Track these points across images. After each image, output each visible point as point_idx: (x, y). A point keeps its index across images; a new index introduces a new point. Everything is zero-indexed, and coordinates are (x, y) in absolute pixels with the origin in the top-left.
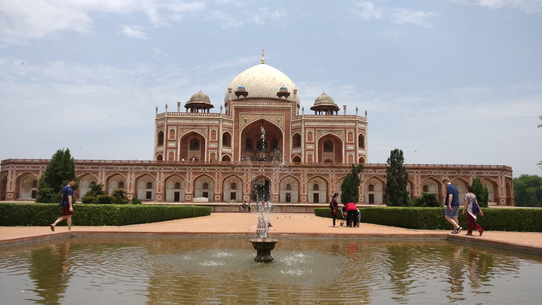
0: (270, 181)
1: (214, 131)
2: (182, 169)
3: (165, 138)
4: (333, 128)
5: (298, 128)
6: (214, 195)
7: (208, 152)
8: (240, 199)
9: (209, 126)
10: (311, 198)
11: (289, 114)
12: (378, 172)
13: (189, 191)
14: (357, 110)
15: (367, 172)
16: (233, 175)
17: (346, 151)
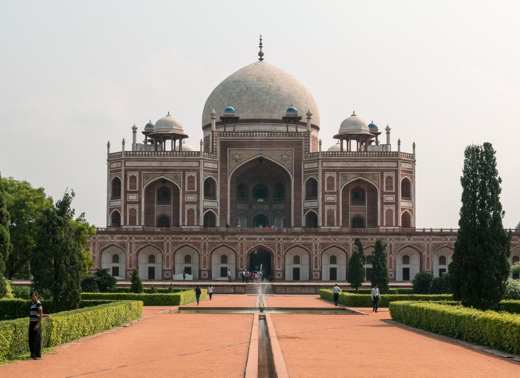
0: (273, 253)
1: (191, 177)
2: (159, 239)
3: (122, 188)
4: (365, 171)
5: (313, 171)
6: (200, 271)
8: (233, 276)
9: (184, 171)
10: (326, 274)
11: (301, 149)
12: (414, 240)
13: (168, 266)
15: (399, 239)
16: (224, 245)
17: (383, 203)
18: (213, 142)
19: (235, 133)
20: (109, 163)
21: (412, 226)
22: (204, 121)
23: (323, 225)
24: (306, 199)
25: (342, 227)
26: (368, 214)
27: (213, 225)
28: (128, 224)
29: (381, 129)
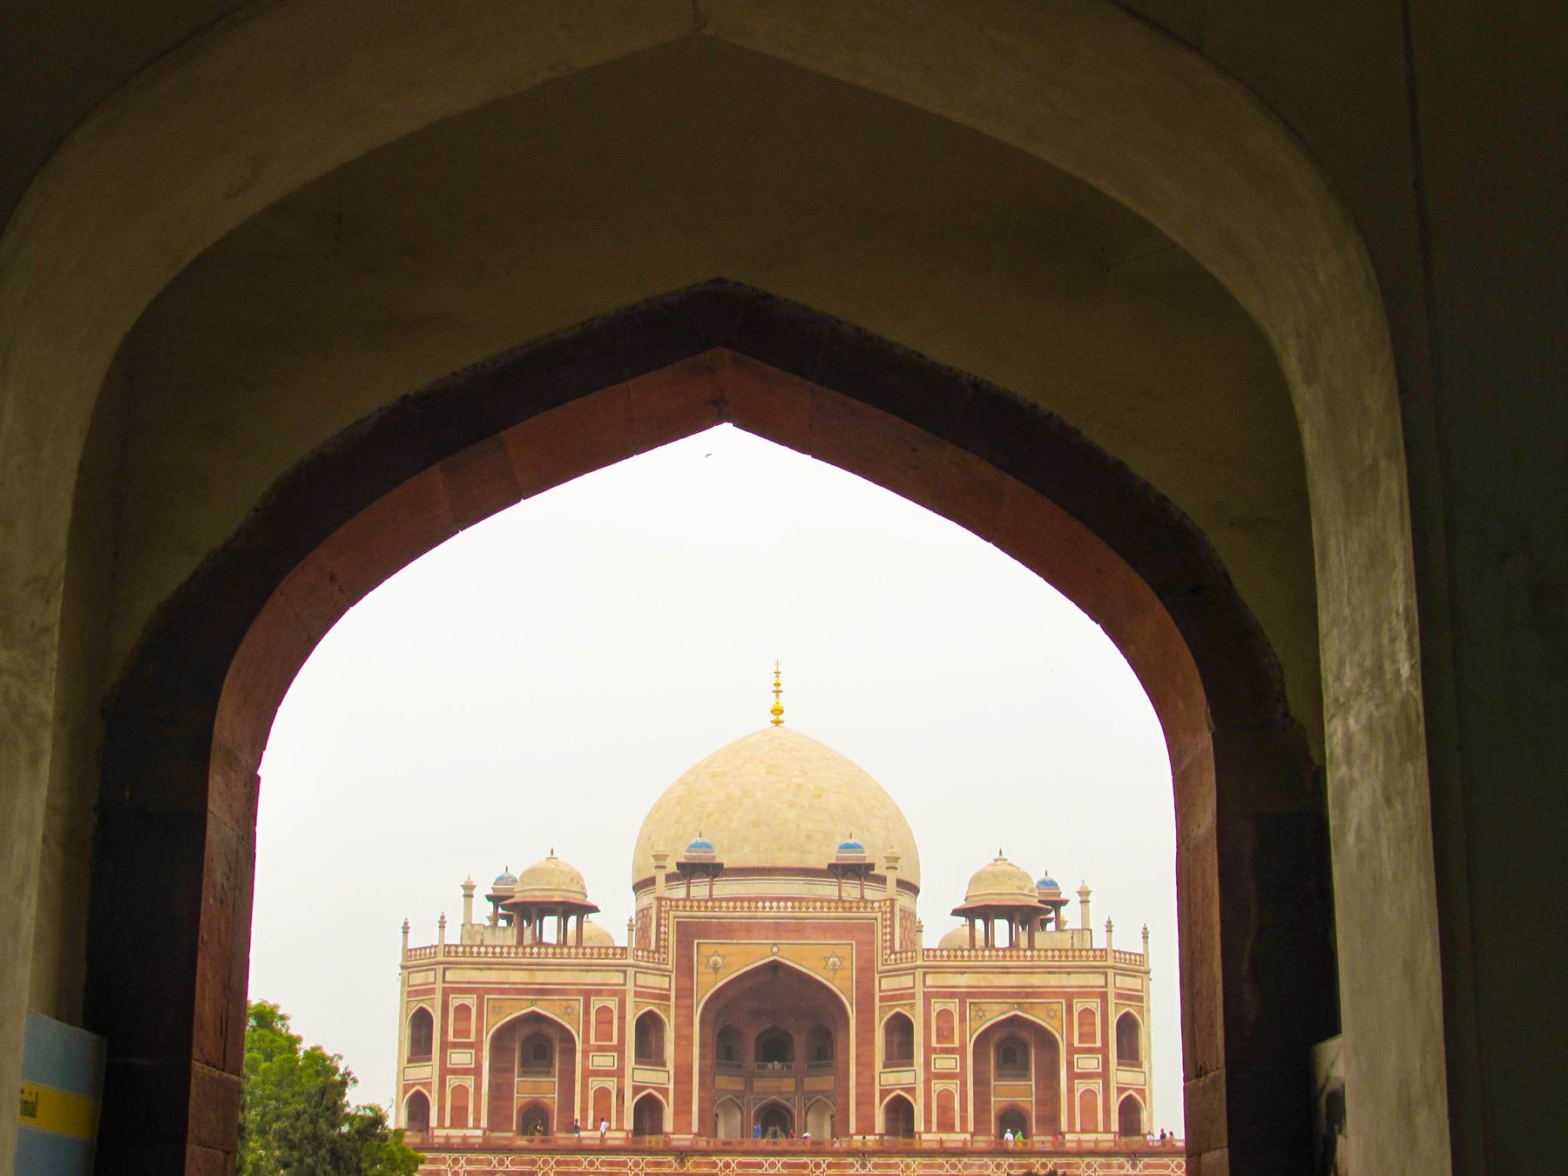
4: (1028, 995)
5: (902, 997)
7: (585, 1086)
9: (587, 994)
11: (871, 943)
14: (1109, 927)
17: (1072, 1076)
18: (659, 925)
19: (714, 900)
20: (406, 972)
21: (1145, 1129)
22: (637, 870)
23: (928, 1130)
24: (885, 1066)
25: (973, 1135)
26: (1038, 1102)
27: (657, 1128)
28: (447, 1123)
29: (1068, 891)
